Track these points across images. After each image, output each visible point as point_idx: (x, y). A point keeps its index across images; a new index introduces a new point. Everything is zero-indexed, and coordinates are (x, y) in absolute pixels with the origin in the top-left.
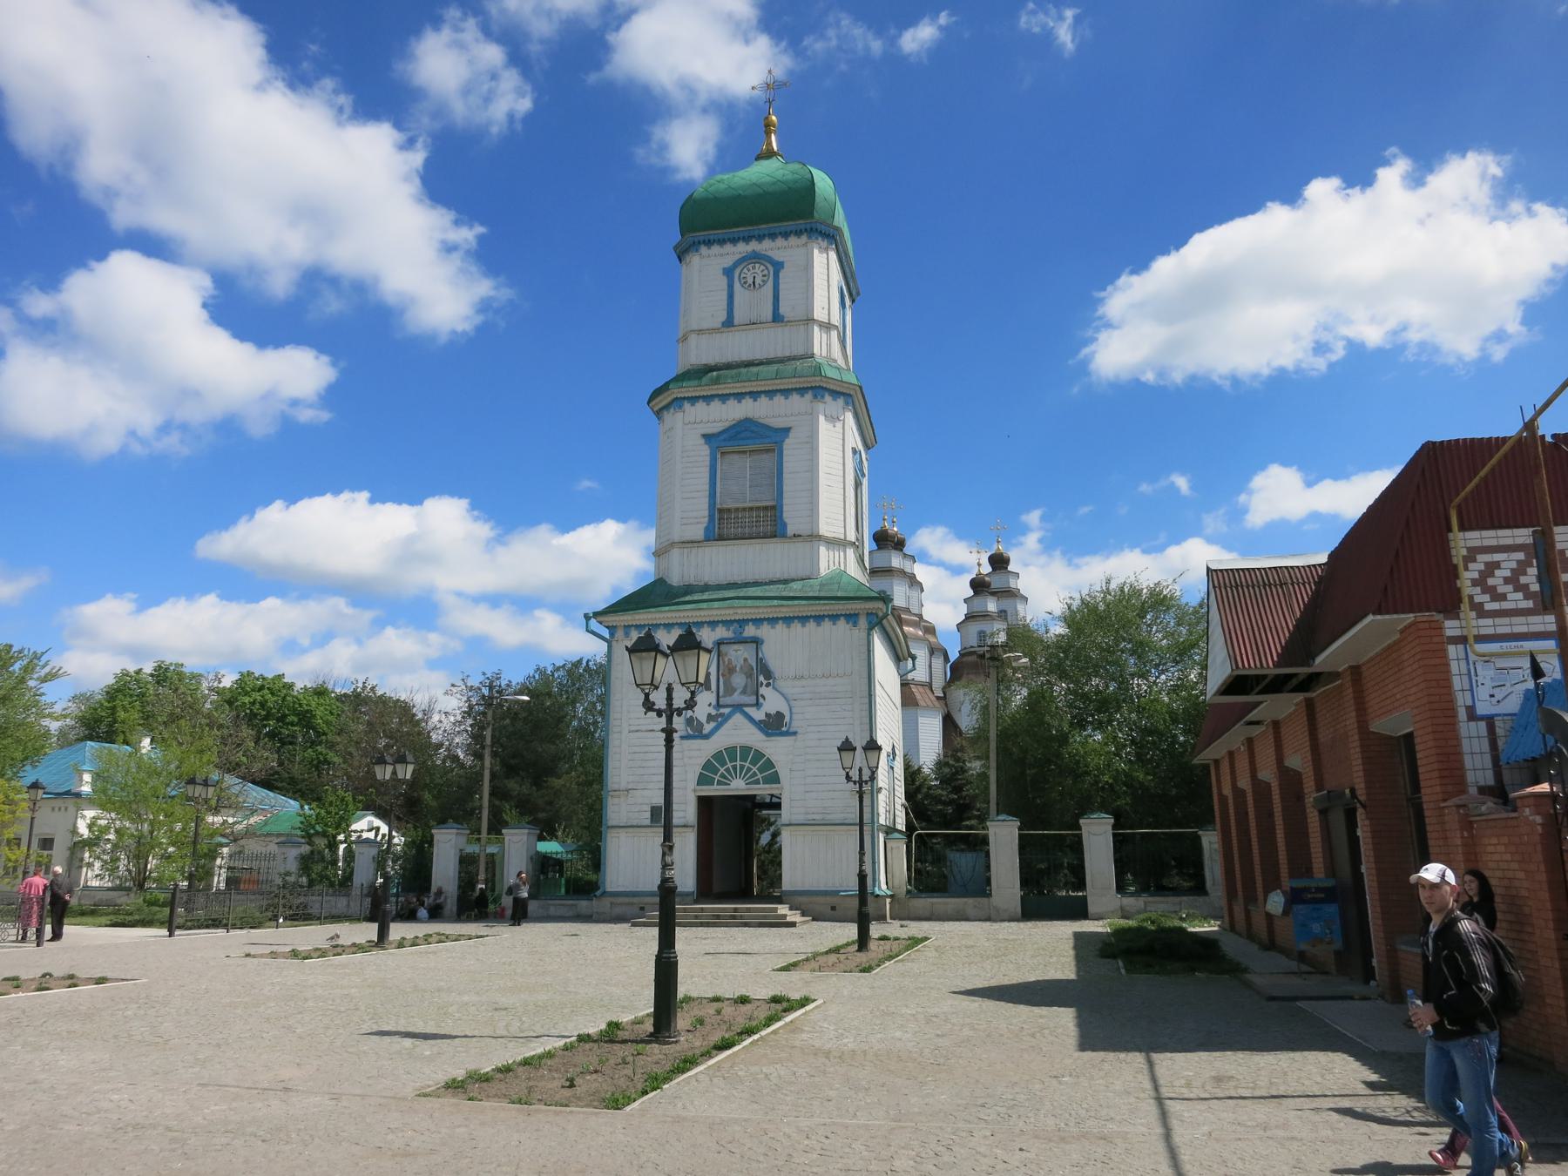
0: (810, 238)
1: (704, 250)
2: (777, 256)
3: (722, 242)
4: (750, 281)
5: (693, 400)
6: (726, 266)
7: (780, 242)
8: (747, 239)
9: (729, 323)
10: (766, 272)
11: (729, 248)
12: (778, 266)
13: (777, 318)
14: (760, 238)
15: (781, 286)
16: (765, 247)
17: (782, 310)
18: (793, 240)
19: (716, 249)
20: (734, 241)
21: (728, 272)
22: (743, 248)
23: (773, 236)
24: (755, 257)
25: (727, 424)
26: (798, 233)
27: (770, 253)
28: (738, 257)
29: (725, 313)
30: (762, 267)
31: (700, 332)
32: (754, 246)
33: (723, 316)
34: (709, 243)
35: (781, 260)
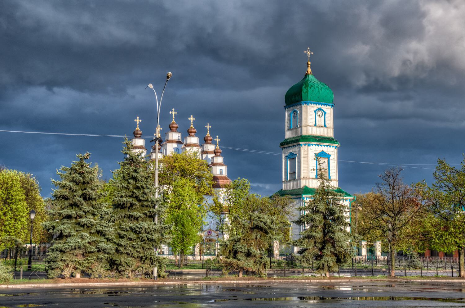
0: (331, 107)
1: (310, 104)
2: (325, 110)
3: (314, 104)
4: (319, 115)
5: (312, 145)
6: (315, 110)
7: (325, 106)
8: (319, 104)
9: (315, 125)
10: (322, 113)
11: (315, 105)
12: (325, 113)
13: (325, 126)
14: (322, 105)
15: (326, 118)
16: (322, 107)
17: (326, 124)
18: (328, 106)
19: (312, 105)
20: (316, 104)
21: (315, 112)
22: (318, 106)
23: (324, 105)
24: (320, 109)
25: (319, 152)
26: (329, 105)
27: (323, 109)
28: (317, 108)
29: (315, 122)
30: (321, 112)
31: (311, 126)
32: (320, 106)
33: (315, 124)
34: (311, 103)
35: (326, 111)
